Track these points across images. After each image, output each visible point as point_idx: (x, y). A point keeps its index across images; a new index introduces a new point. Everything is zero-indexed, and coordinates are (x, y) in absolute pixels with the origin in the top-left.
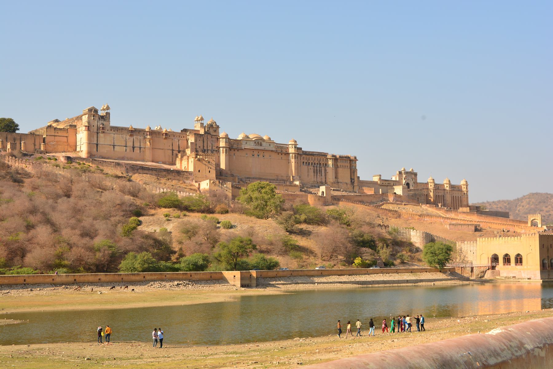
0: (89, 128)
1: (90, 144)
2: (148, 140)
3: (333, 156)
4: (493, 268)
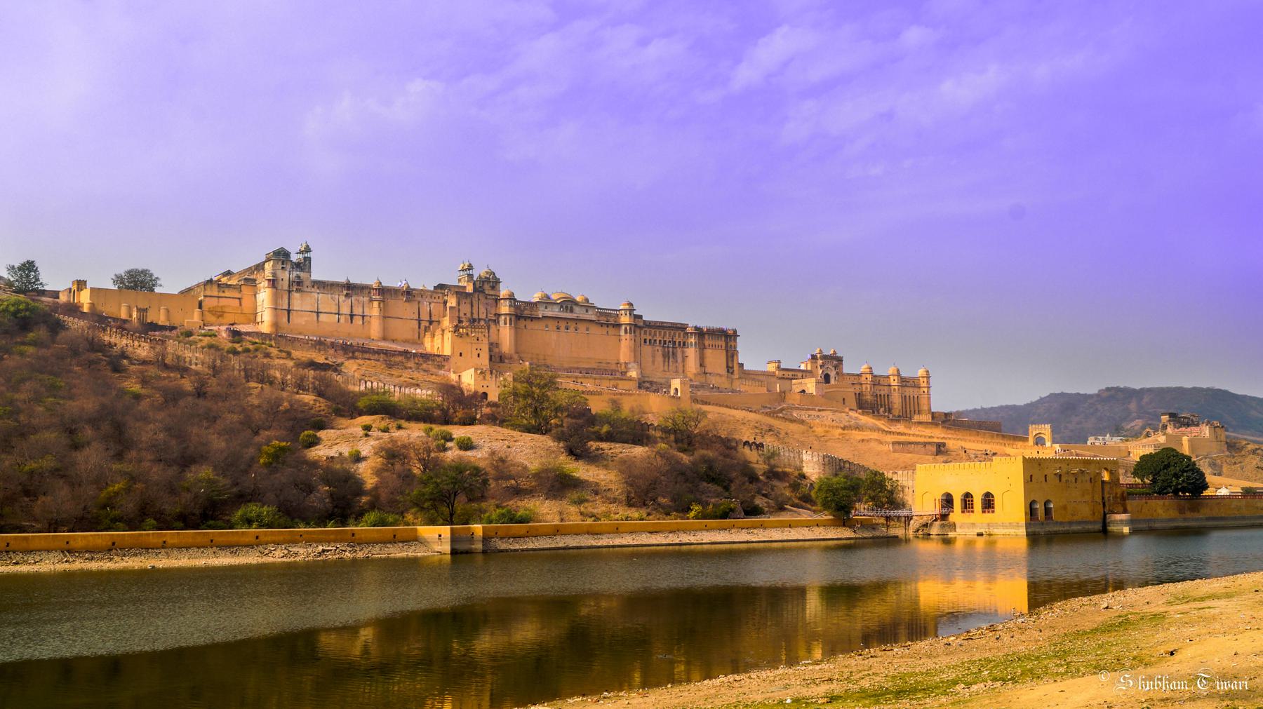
0: (273, 283)
3: (696, 328)
4: (944, 517)
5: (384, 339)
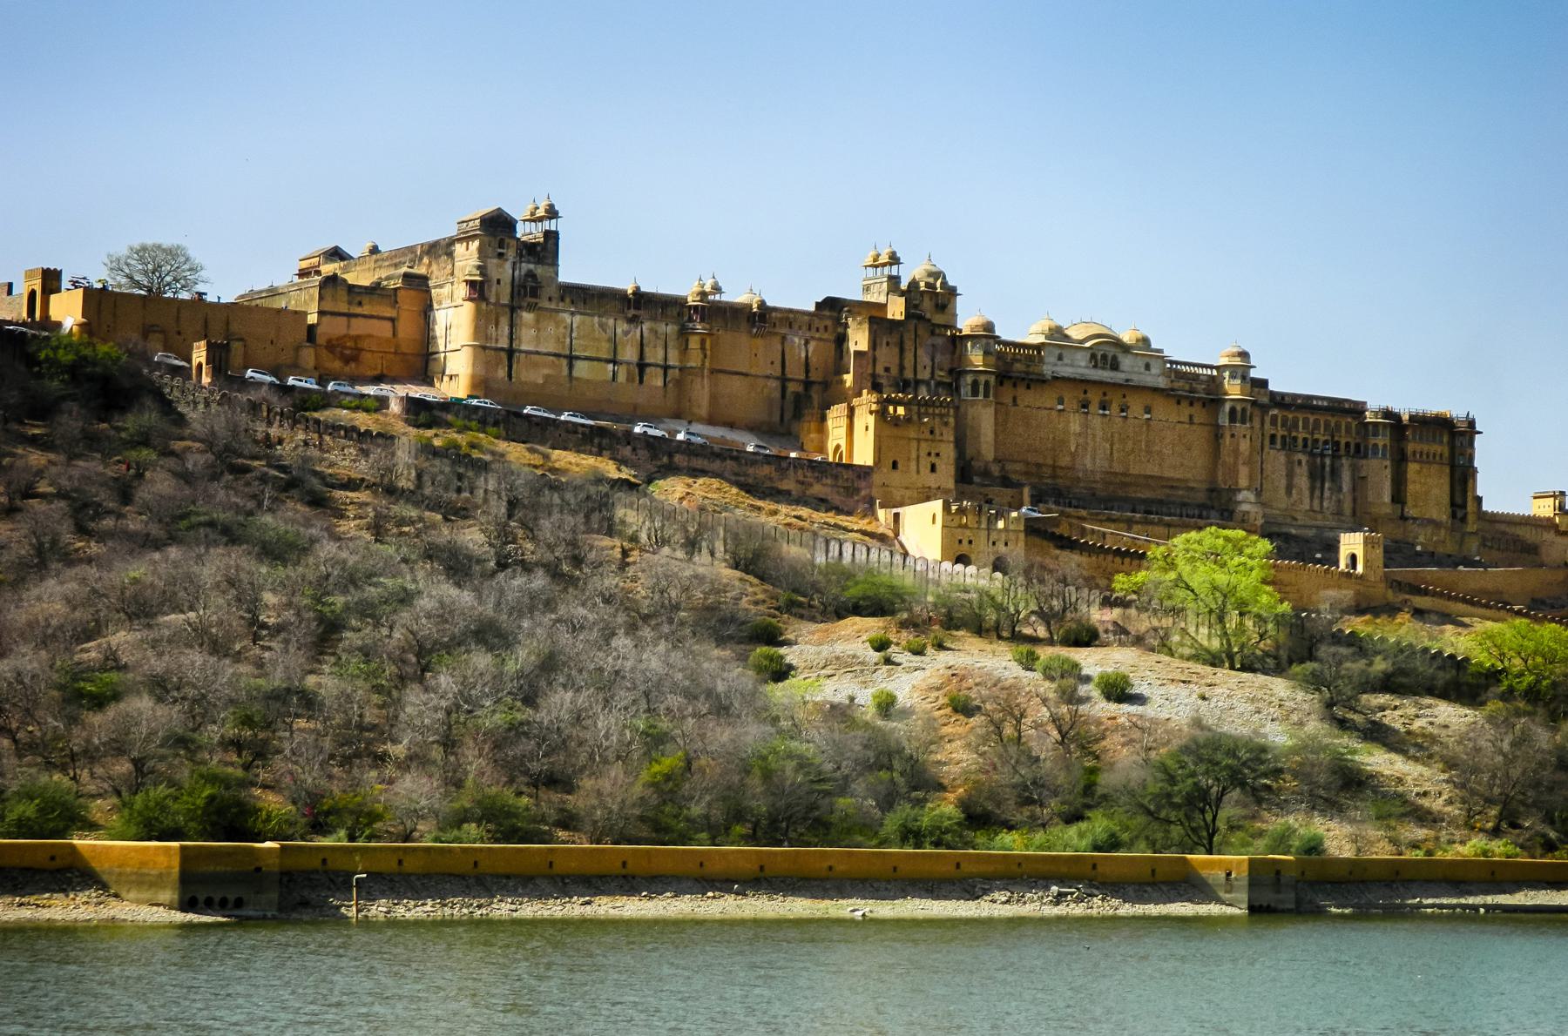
0: (478, 290)
1: (483, 348)
3: (1388, 414)
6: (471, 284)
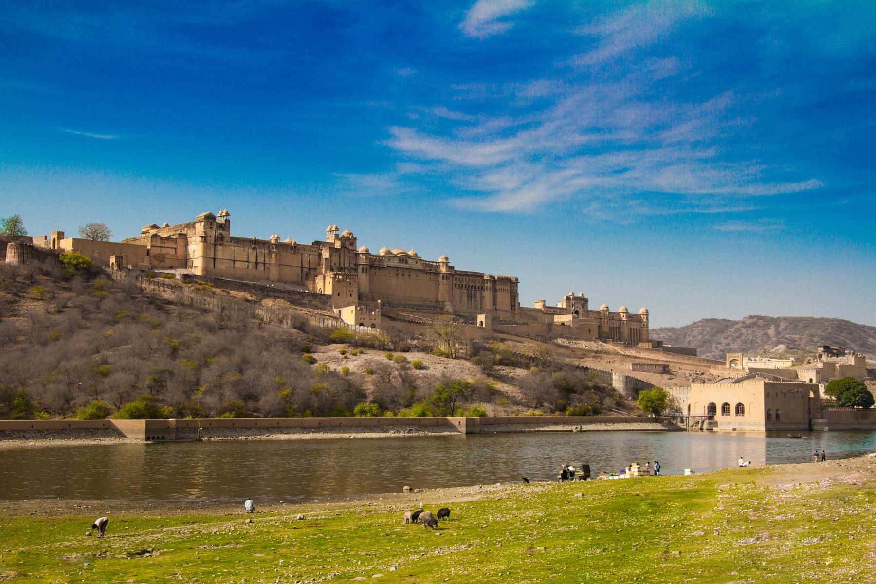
0: (204, 239)
1: (206, 258)
2: (273, 255)
3: (491, 277)
4: (711, 418)
5: (279, 281)
6: (202, 237)
